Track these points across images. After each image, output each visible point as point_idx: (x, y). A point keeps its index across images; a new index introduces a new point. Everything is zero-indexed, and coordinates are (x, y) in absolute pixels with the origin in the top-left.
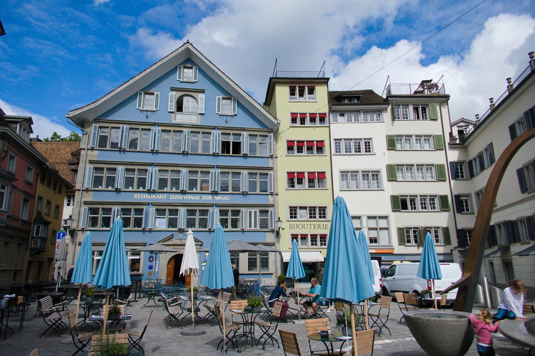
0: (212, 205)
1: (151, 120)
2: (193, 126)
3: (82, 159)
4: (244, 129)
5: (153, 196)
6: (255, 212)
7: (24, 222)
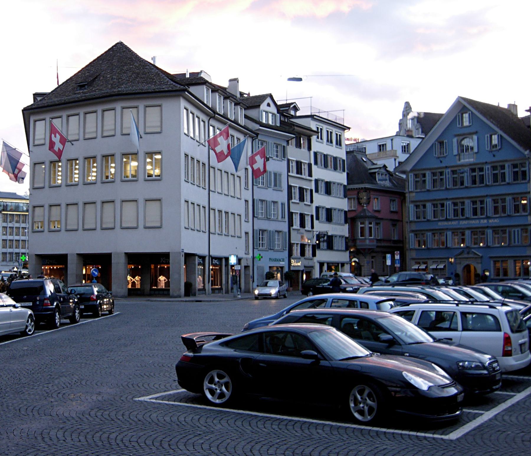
0: (487, 227)
1: (443, 165)
2: (471, 165)
3: (408, 200)
4: (506, 161)
5: (450, 223)
6: (518, 231)
7: (395, 242)
